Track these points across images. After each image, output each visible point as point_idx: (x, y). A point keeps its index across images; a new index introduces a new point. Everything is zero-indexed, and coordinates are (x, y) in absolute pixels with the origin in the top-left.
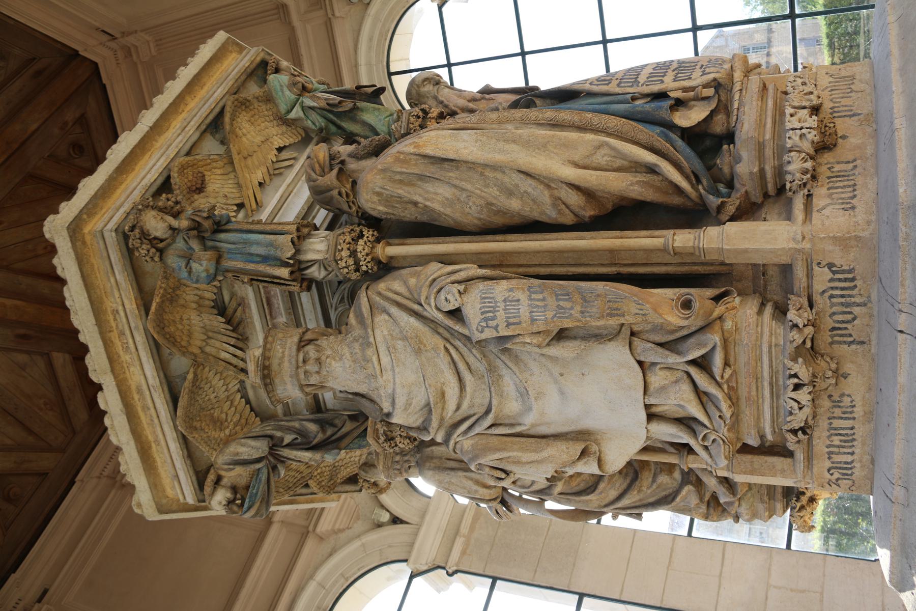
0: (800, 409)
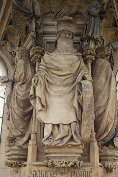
0: (60, 164)
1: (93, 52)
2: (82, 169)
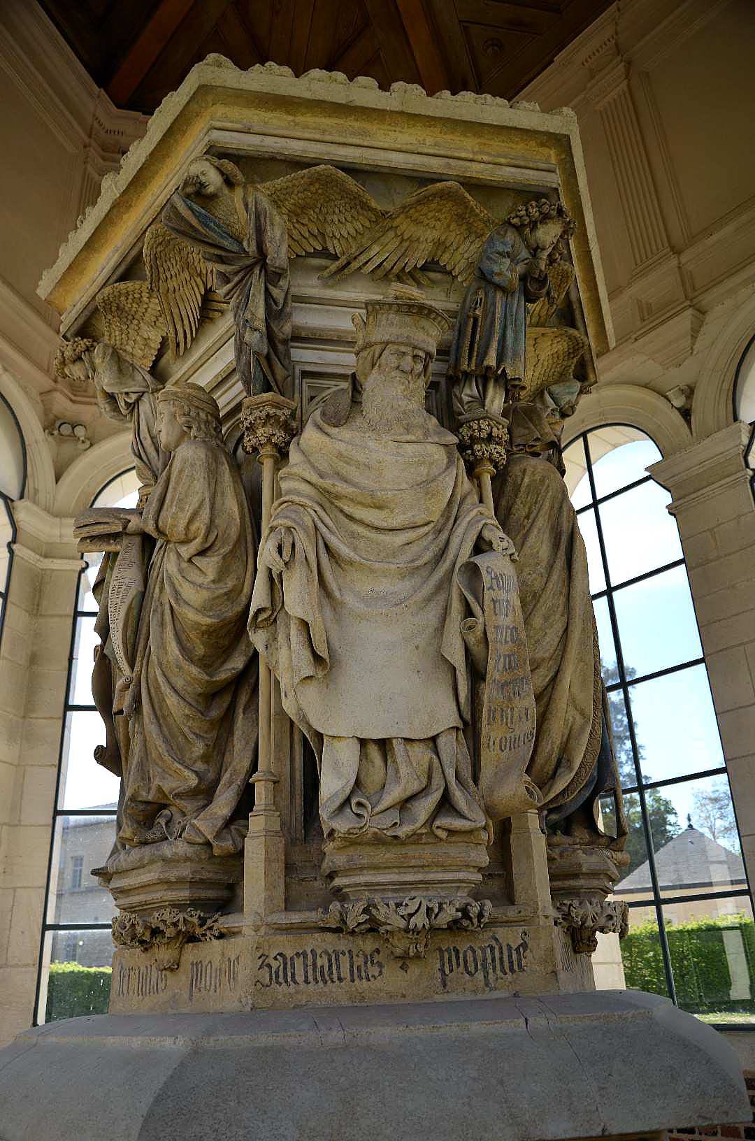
1: (501, 432)
2: (485, 938)
